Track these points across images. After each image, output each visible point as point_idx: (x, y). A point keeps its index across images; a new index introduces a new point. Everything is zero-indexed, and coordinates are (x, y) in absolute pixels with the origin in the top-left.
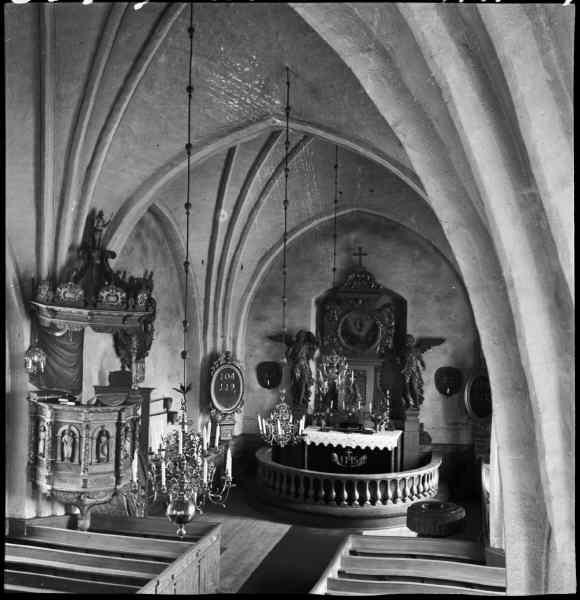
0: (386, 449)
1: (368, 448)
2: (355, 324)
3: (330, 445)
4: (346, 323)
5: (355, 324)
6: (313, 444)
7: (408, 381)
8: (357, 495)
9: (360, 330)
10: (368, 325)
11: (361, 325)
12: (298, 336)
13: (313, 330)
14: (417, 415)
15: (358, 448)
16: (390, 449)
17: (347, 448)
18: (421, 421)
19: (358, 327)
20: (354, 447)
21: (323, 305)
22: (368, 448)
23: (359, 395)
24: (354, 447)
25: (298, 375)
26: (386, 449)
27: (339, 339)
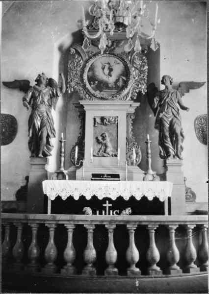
0: (156, 199)
1: (132, 198)
2: (103, 68)
3: (82, 198)
4: (92, 69)
5: (103, 68)
6: (58, 198)
7: (167, 126)
8: (156, 253)
9: (110, 75)
10: (118, 69)
11: (111, 70)
12: (39, 81)
13: (55, 77)
14: (180, 165)
15: (120, 198)
16: (161, 200)
17: (105, 199)
18: (185, 176)
19: (107, 71)
20: (114, 198)
21: (66, 55)
22: (132, 198)
23: (109, 144)
24: (114, 198)
25: (38, 123)
26: (156, 199)
27: (84, 87)
